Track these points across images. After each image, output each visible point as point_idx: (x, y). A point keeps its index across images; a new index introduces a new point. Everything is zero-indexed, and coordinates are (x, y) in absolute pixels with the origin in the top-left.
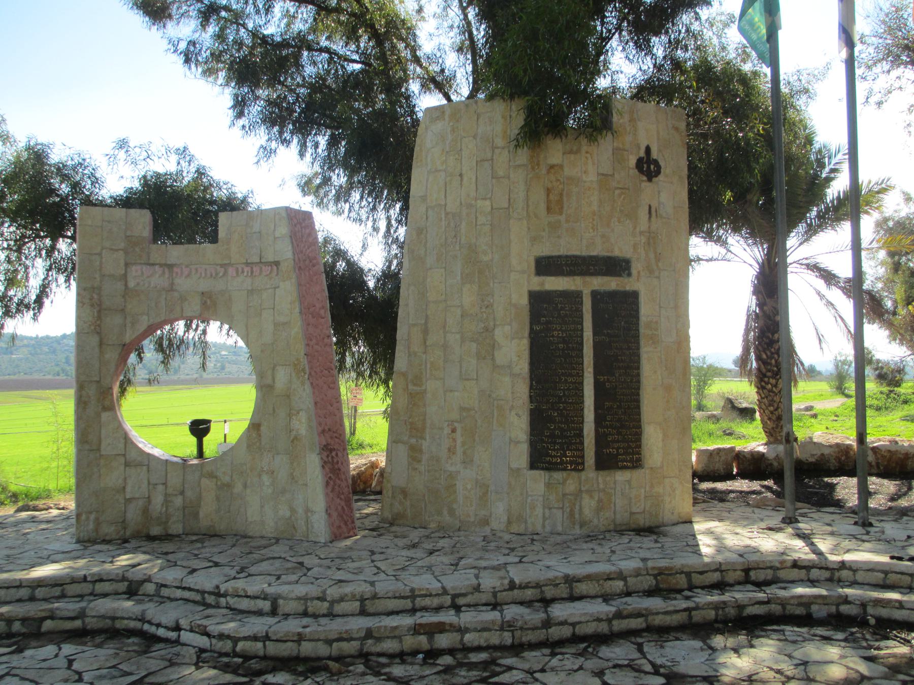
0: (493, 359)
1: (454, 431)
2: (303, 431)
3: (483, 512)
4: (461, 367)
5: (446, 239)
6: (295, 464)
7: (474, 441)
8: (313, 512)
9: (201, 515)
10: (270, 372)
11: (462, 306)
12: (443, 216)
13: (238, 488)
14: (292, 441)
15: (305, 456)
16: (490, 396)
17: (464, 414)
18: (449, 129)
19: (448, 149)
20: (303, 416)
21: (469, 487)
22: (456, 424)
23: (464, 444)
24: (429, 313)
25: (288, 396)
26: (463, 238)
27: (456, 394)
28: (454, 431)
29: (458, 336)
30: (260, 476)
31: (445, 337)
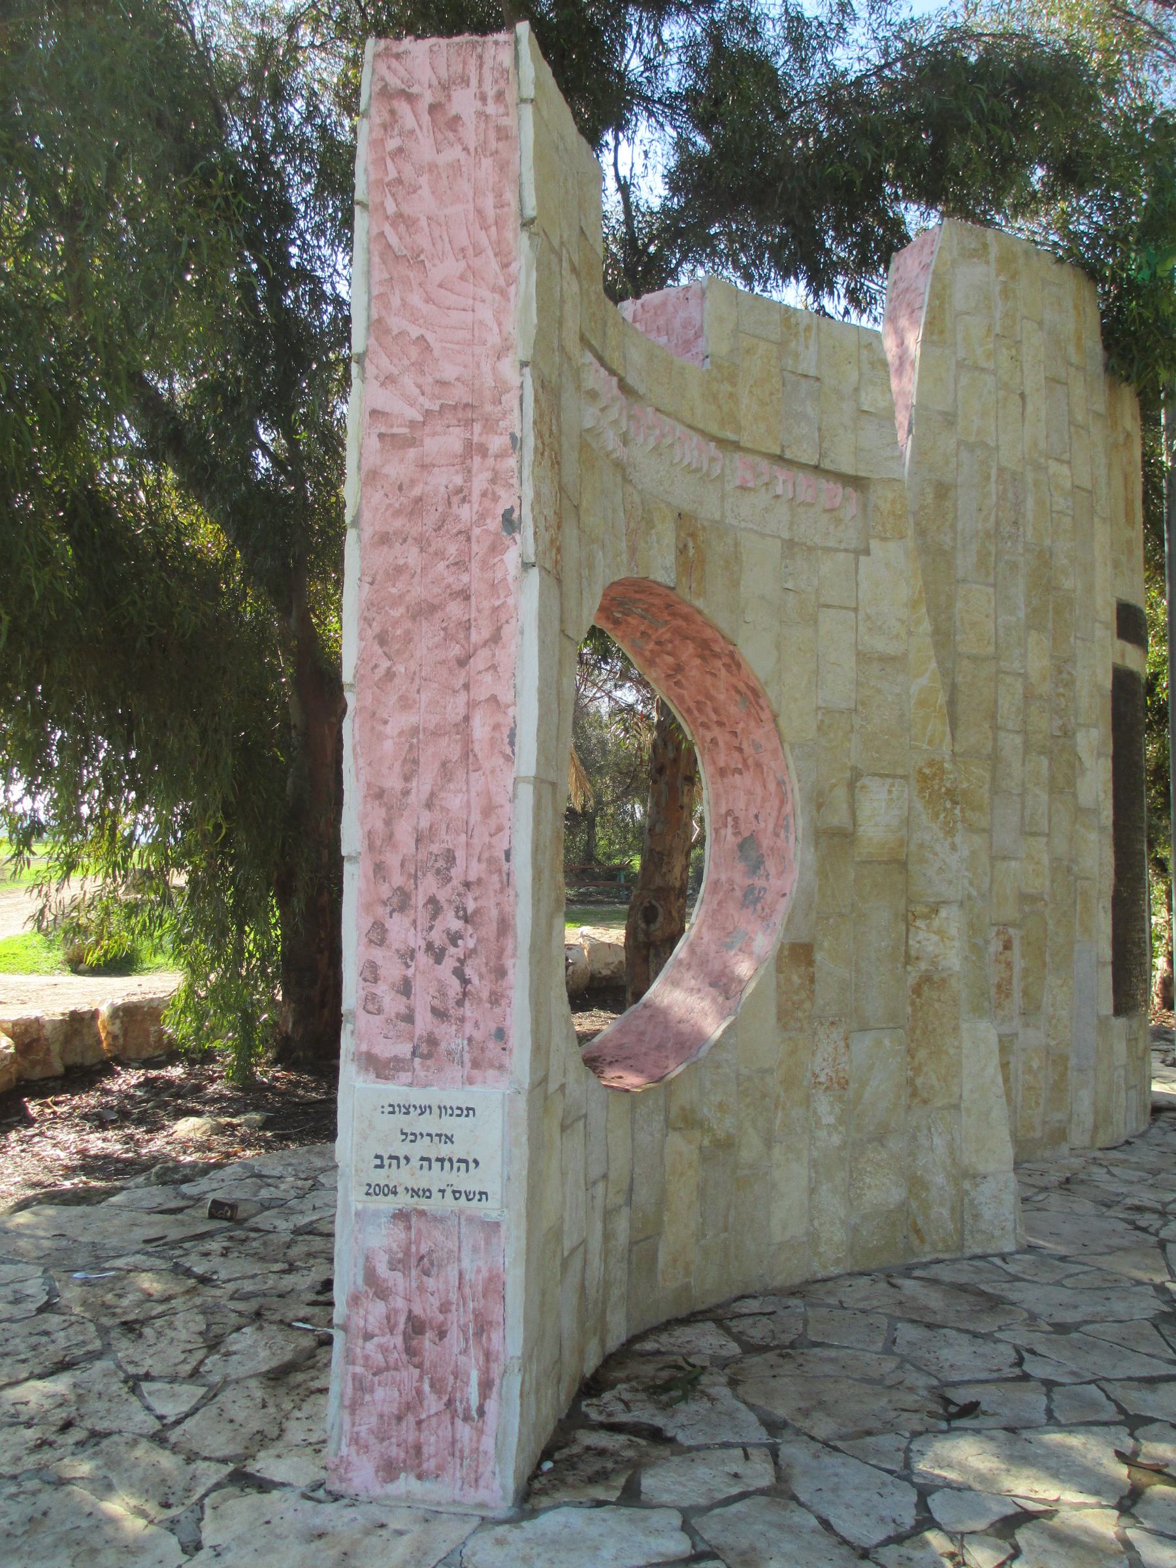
0: (1075, 795)
1: (1007, 946)
2: (953, 959)
3: (1059, 1116)
4: (1023, 808)
5: (997, 523)
6: (922, 1054)
7: (1044, 964)
8: (977, 1178)
9: (663, 1258)
10: (841, 793)
11: (1025, 676)
12: (994, 472)
13: (750, 1149)
14: (917, 990)
15: (956, 1029)
16: (1069, 870)
17: (1027, 909)
18: (998, 289)
19: (998, 329)
20: (951, 919)
21: (1035, 1064)
22: (1011, 931)
23: (1026, 972)
24: (959, 679)
25: (903, 865)
26: (1029, 533)
27: (1013, 863)
28: (1007, 946)
29: (1018, 740)
30: (808, 1100)
31: (995, 740)
